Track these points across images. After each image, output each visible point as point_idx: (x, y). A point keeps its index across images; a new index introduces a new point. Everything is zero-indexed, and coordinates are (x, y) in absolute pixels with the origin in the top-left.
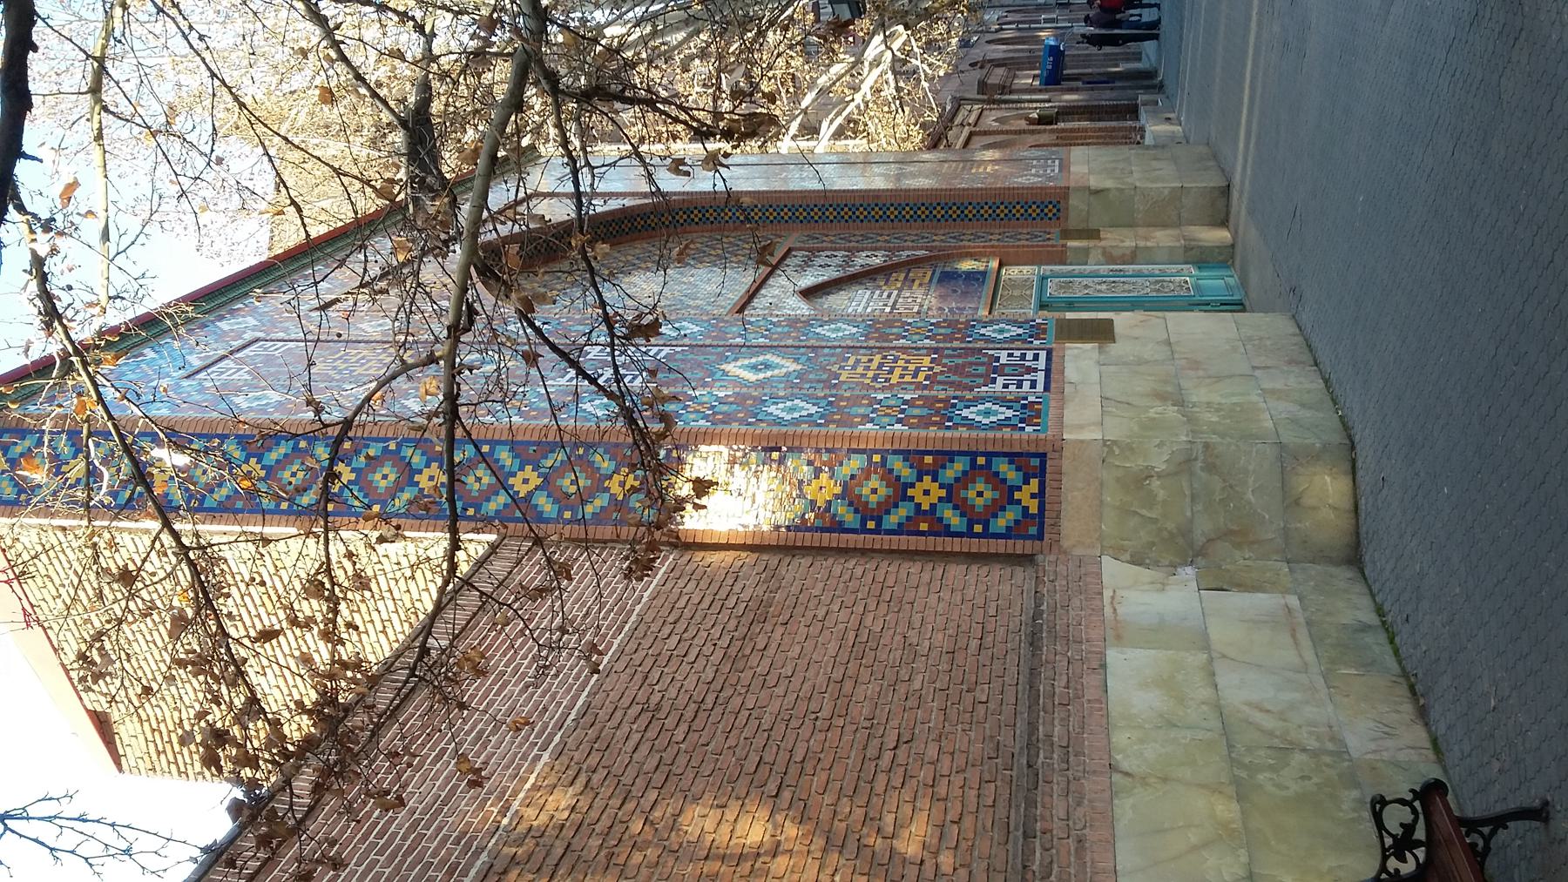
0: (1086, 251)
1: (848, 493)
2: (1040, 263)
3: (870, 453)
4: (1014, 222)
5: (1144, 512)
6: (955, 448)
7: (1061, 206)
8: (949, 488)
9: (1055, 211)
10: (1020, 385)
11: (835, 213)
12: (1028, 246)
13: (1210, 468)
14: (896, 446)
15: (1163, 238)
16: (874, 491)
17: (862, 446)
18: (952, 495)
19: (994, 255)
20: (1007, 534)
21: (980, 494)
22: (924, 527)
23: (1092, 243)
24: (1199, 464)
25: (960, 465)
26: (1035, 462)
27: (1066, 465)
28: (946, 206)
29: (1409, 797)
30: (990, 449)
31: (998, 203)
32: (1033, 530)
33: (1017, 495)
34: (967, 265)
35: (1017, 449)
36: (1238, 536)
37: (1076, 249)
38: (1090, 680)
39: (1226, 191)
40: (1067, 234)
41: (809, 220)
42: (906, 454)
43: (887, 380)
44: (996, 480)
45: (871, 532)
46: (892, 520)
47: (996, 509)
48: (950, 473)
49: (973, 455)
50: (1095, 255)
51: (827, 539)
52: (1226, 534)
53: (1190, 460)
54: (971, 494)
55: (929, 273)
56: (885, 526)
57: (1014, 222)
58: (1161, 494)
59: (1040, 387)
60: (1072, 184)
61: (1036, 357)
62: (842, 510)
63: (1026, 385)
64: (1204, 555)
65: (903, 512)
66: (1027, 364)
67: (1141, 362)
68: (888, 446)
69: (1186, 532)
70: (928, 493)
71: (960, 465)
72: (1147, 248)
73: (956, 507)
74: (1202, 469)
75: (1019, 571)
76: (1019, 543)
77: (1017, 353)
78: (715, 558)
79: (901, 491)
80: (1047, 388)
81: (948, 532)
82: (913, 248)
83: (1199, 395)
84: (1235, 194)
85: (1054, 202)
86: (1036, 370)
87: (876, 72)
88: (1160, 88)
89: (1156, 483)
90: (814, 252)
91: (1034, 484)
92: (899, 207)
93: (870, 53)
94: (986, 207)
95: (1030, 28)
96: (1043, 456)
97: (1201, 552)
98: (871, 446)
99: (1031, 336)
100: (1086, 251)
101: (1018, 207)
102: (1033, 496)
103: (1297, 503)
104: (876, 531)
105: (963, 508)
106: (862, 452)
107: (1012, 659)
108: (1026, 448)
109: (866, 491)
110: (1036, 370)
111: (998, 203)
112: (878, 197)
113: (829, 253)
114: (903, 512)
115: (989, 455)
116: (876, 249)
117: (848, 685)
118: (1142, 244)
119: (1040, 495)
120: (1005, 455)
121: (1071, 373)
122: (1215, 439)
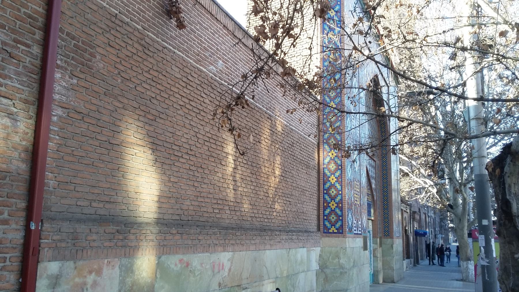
0: (377, 244)
1: (332, 186)
2: (373, 231)
3: (341, 190)
5: (331, 257)
6: (343, 212)
7: (388, 236)
8: (334, 210)
10: (355, 227)
15: (380, 265)
16: (333, 192)
17: (343, 189)
18: (333, 211)
19: (375, 218)
20: (324, 225)
21: (333, 218)
22: (325, 204)
23: (378, 245)
24: (342, 270)
25: (339, 213)
26: (341, 231)
27: (340, 239)
28: (387, 205)
30: (343, 220)
32: (325, 231)
33: (333, 227)
34: (372, 211)
36: (326, 279)
38: (301, 245)
39: (393, 282)
40: (381, 238)
41: (383, 166)
42: (341, 200)
44: (336, 222)
45: (324, 192)
46: (326, 197)
47: (330, 222)
48: (337, 210)
49: (342, 216)
50: (375, 246)
51: (321, 181)
52: (326, 277)
53: (343, 268)
54: (333, 216)
56: (325, 195)
58: (335, 261)
59: (355, 232)
60: (394, 239)
61: (360, 231)
62: (328, 184)
64: (322, 272)
65: (329, 199)
67: (360, 257)
68: (343, 195)
69: (326, 267)
70: (333, 205)
71: (339, 213)
72: (378, 260)
73: (330, 212)
75: (316, 228)
76: (322, 228)
78: (316, 154)
79: (333, 199)
80: (355, 234)
81: (324, 210)
82: (376, 196)
83: (355, 271)
84: (393, 284)
87: (422, 183)
88: (415, 265)
89: (337, 260)
90: (375, 168)
91: (336, 231)
92: (387, 192)
93: (427, 181)
95: (429, 226)
97: (322, 271)
98: (343, 191)
100: (377, 244)
102: (333, 231)
104: (324, 193)
105: (330, 214)
107: (302, 226)
108: (344, 229)
109: (333, 190)
114: (329, 199)
115: (342, 220)
116: (376, 185)
117: (297, 189)
118: (379, 259)
119: (334, 233)
120: (342, 224)
121: (358, 239)
122: (348, 274)
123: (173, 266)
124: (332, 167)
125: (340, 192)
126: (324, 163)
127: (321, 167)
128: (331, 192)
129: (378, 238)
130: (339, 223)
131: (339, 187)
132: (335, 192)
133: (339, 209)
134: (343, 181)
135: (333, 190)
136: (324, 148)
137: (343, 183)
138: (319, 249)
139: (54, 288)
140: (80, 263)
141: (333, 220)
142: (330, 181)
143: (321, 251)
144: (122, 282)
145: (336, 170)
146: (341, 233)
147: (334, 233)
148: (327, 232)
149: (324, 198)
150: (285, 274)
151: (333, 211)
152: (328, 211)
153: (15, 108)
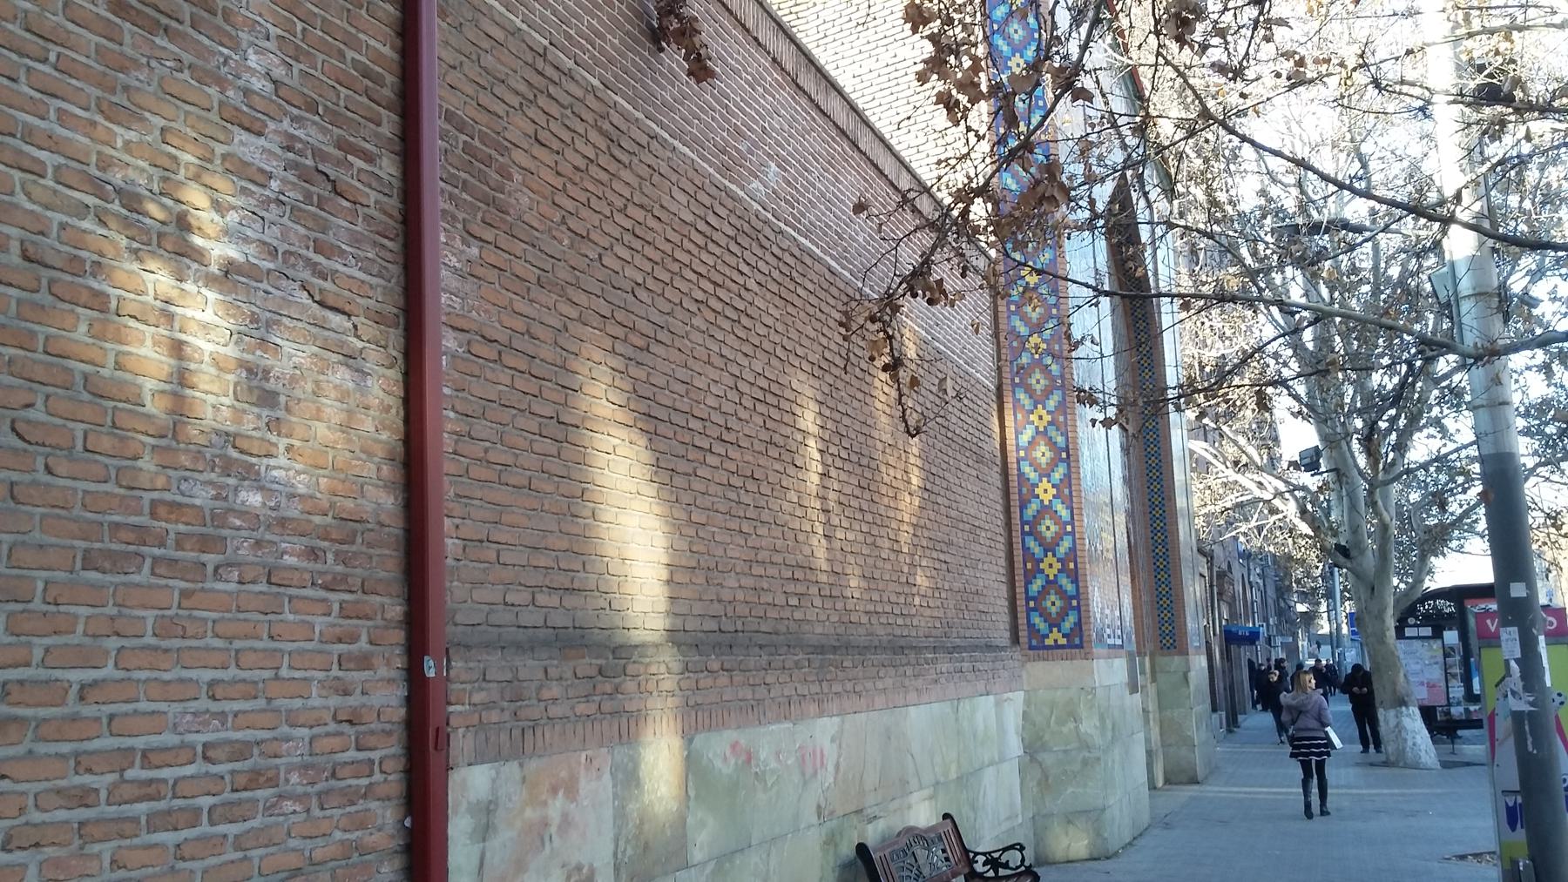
1: (1046, 510)
4: (1157, 612)
7: (1173, 650)
8: (1055, 582)
13: (1085, 762)
16: (1048, 528)
18: (1051, 583)
20: (1030, 625)
21: (1053, 604)
22: (1029, 566)
23: (1148, 675)
24: (1087, 755)
26: (1077, 641)
28: (1166, 557)
29: (1027, 863)
30: (1083, 609)
32: (1034, 642)
33: (1055, 629)
36: (1045, 783)
38: (981, 686)
39: (1194, 781)
42: (1073, 550)
44: (1063, 614)
45: (1023, 528)
46: (1031, 543)
47: (1045, 615)
48: (1064, 581)
49: (1077, 596)
51: (1015, 497)
53: (1088, 748)
54: (1053, 598)
56: (1027, 538)
58: (1065, 730)
59: (1110, 641)
60: (1191, 657)
62: (1033, 507)
64: (1031, 761)
65: (1037, 550)
68: (1077, 536)
69: (1044, 748)
70: (1051, 566)
75: (1007, 634)
76: (1026, 633)
78: (995, 420)
79: (1049, 547)
83: (1117, 752)
84: (1196, 787)
87: (1253, 486)
88: (1230, 731)
89: (1072, 725)
91: (1063, 641)
92: (1162, 518)
93: (1266, 478)
95: (1253, 613)
97: (1033, 759)
102: (1056, 641)
103: (1069, 822)
104: (1023, 533)
105: (1044, 592)
106: (1072, 518)
107: (976, 633)
108: (1086, 633)
109: (1048, 522)
112: (1170, 499)
114: (1037, 550)
115: (1078, 608)
117: (961, 526)
119: (1057, 646)
120: (1080, 619)
123: (718, 763)
124: (1042, 453)
125: (1069, 528)
126: (1017, 445)
127: (1012, 458)
128: (1043, 528)
129: (1145, 654)
130: (1072, 619)
131: (1064, 513)
132: (1053, 528)
133: (1068, 577)
135: (1048, 522)
136: (1017, 401)
138: (1019, 696)
139: (484, 840)
140: (533, 765)
141: (1053, 610)
142: (1037, 496)
143: (1027, 702)
144: (620, 815)
145: (1053, 464)
146: (1076, 647)
147: (1057, 646)
148: (1038, 647)
149: (1026, 549)
150: (953, 775)
151: (1051, 583)
152: (1036, 586)
153: (358, 337)
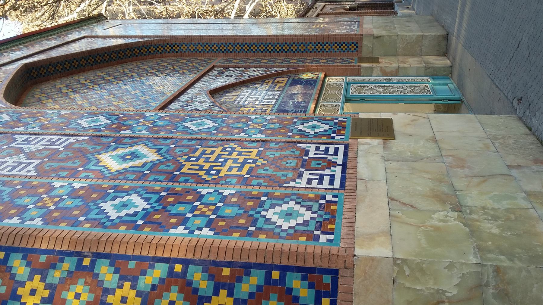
2: (346, 75)
4: (333, 53)
6: (252, 260)
9: (355, 47)
10: (321, 182)
11: (240, 48)
12: (340, 66)
14: (197, 257)
15: (413, 62)
17: (167, 255)
19: (322, 70)
23: (374, 65)
26: (327, 279)
27: (358, 284)
30: (285, 262)
31: (325, 43)
34: (307, 76)
35: (309, 264)
37: (366, 68)
39: (447, 37)
40: (361, 60)
41: (227, 51)
43: (219, 172)
49: (268, 268)
50: (376, 71)
55: (286, 81)
57: (333, 53)
59: (337, 184)
60: (364, 33)
61: (336, 152)
63: (327, 179)
66: (329, 158)
67: (417, 158)
68: (190, 256)
72: (405, 67)
74: (494, 296)
77: (323, 147)
80: (343, 186)
82: (279, 67)
84: (453, 39)
85: (355, 43)
86: (335, 164)
90: (226, 68)
94: (319, 45)
96: (334, 273)
98: (174, 255)
99: (334, 132)
100: (372, 69)
101: (336, 45)
110: (335, 164)
111: (325, 43)
112: (262, 39)
113: (233, 69)
115: (284, 269)
116: (259, 67)
118: (402, 65)
120: (299, 269)
121: (363, 170)
122: (504, 262)
125: (178, 268)
129: (359, 66)
134: (137, 253)
137: (144, 253)
146: (335, 282)
